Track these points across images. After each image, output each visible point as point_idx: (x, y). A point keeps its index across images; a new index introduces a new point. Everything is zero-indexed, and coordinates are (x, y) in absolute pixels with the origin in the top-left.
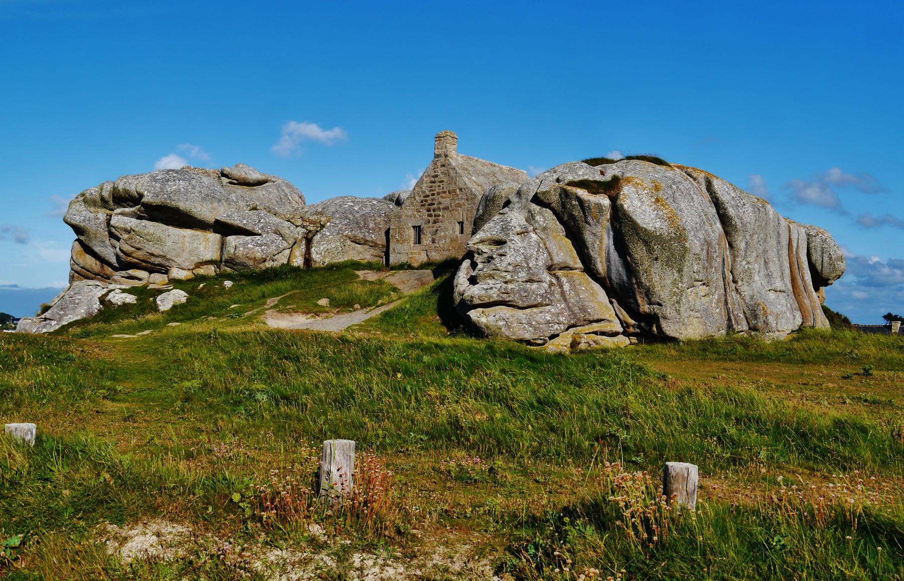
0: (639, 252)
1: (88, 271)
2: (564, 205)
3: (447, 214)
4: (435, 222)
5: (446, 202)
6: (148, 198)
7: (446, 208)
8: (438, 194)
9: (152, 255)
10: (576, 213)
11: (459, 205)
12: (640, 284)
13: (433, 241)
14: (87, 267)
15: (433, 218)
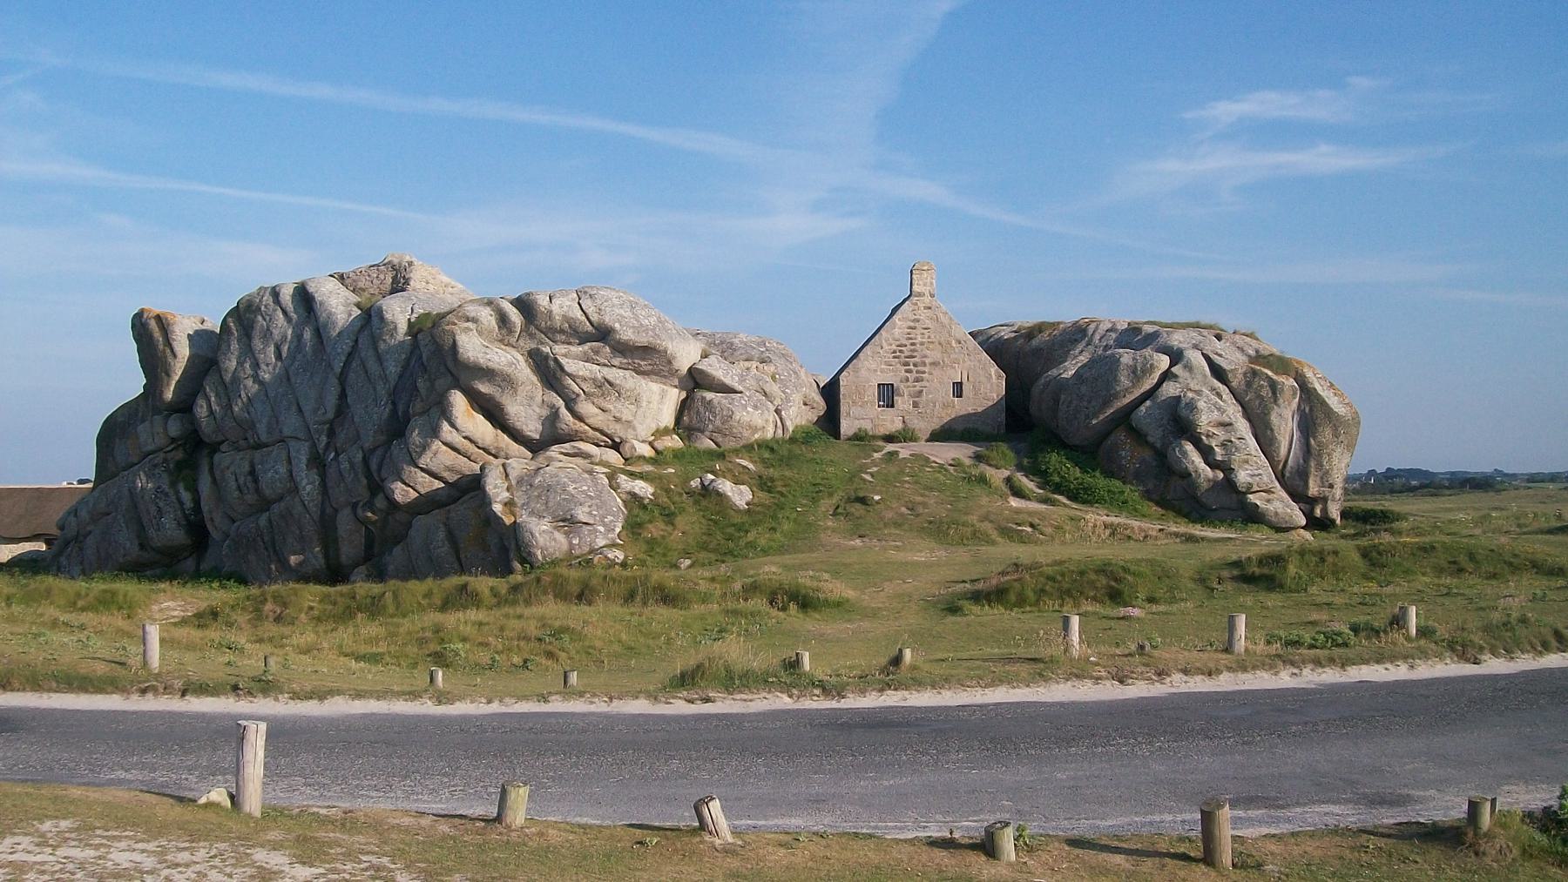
0: (1326, 434)
1: (471, 441)
2: (1249, 384)
3: (937, 372)
4: (917, 380)
5: (934, 354)
6: (626, 334)
7: (934, 364)
8: (922, 344)
9: (618, 420)
10: (1263, 393)
11: (956, 361)
12: (1320, 465)
13: (915, 405)
14: (477, 436)
15: (915, 375)
